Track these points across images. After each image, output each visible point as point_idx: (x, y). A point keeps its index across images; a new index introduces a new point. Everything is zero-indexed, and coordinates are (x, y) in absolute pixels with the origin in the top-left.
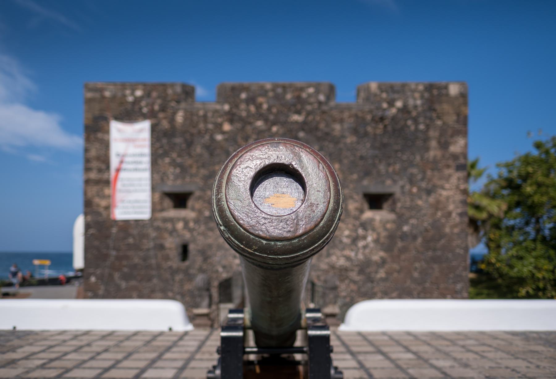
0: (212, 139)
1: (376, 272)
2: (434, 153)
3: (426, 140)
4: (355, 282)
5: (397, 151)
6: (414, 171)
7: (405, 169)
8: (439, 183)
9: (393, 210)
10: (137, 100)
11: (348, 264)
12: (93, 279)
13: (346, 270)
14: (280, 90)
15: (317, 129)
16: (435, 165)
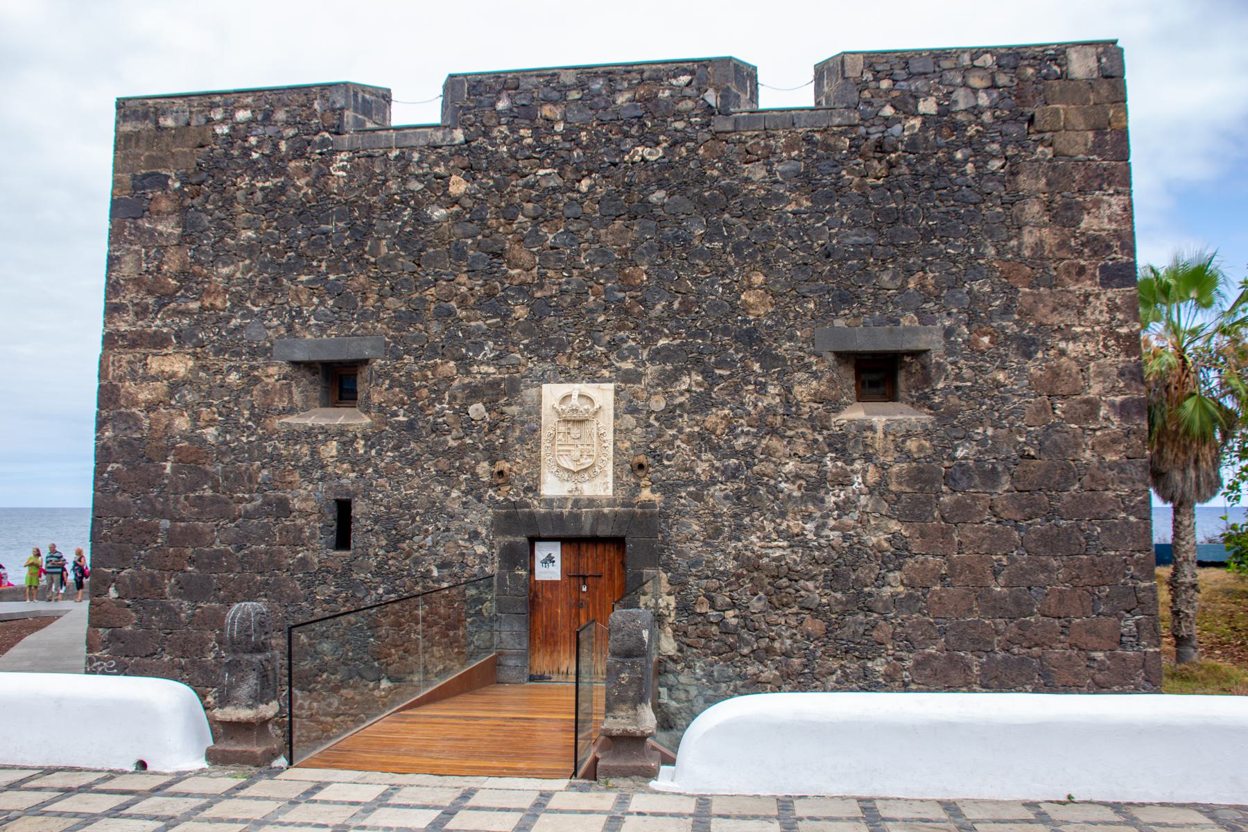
0: (420, 219)
1: (881, 581)
2: (1036, 234)
3: (1014, 199)
4: (816, 612)
5: (927, 234)
6: (981, 287)
7: (955, 283)
8: (1055, 319)
9: (922, 401)
10: (238, 134)
11: (794, 557)
12: (113, 593)
13: (793, 575)
14: (597, 85)
15: (701, 178)
16: (1040, 268)
